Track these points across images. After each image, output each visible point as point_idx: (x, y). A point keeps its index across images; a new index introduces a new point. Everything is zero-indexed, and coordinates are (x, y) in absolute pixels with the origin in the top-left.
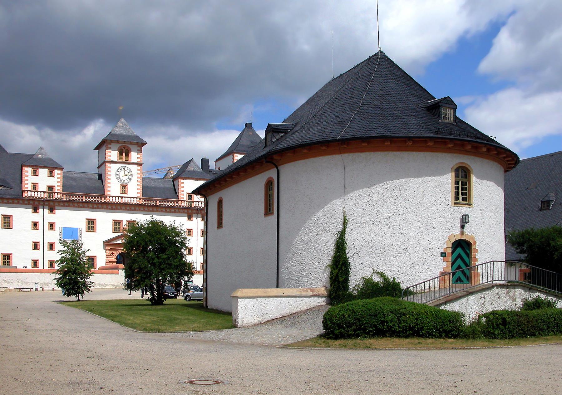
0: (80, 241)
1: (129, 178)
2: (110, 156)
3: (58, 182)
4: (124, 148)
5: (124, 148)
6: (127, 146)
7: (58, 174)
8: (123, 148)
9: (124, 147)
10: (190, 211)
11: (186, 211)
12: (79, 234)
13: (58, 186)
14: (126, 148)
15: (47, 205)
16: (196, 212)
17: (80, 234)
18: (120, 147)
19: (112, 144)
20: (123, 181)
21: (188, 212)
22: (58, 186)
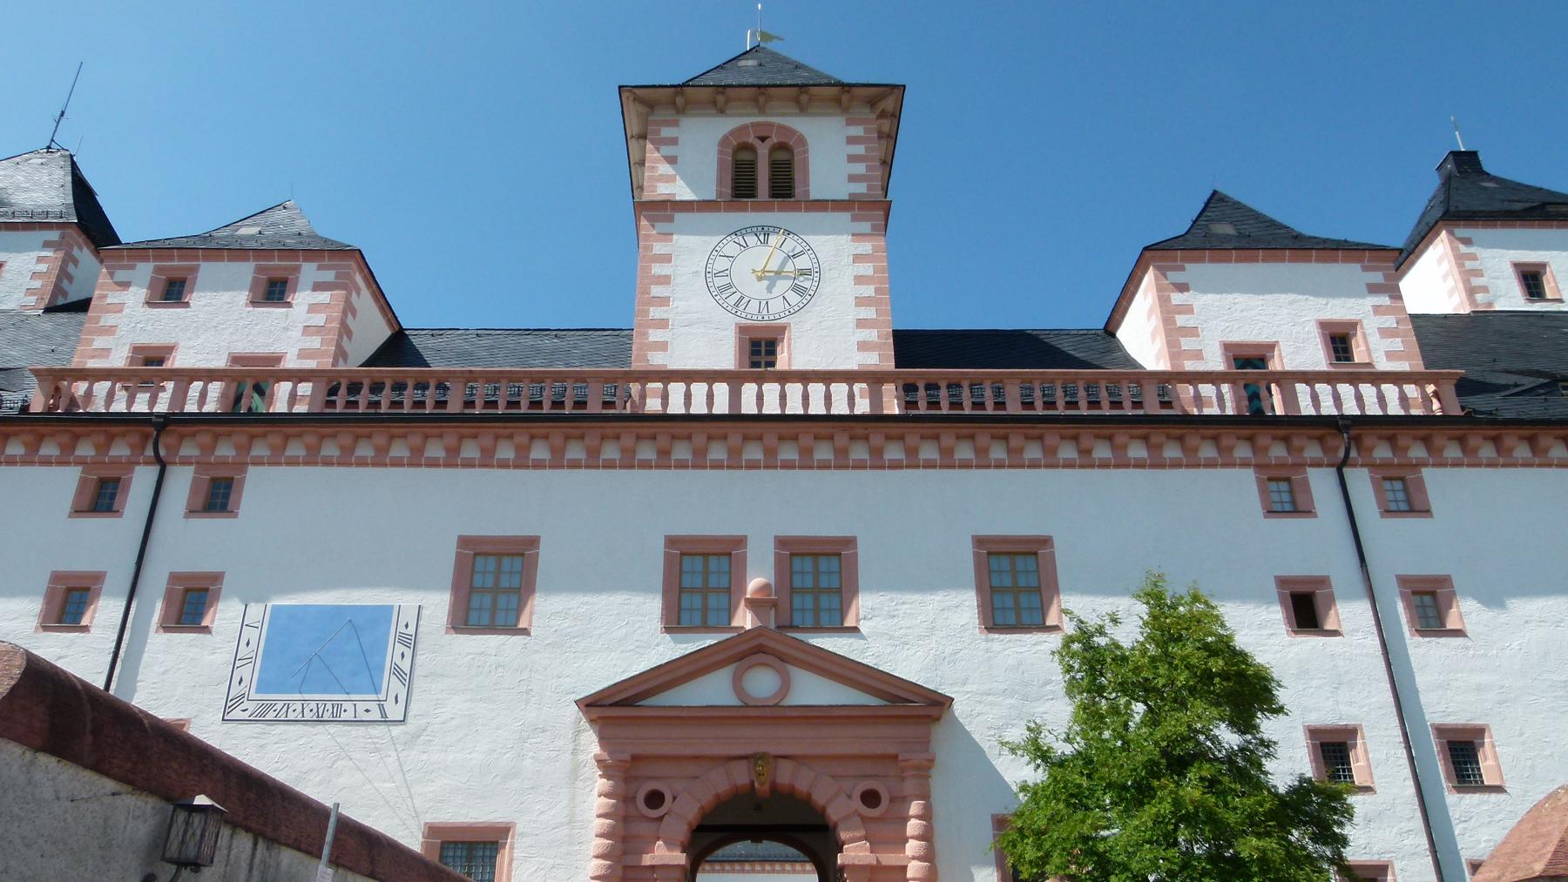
1: (798, 289)
4: (763, 139)
5: (763, 139)
6: (781, 127)
8: (751, 139)
9: (763, 134)
12: (395, 653)
14: (775, 140)
15: (186, 462)
17: (400, 648)
18: (732, 133)
20: (753, 307)
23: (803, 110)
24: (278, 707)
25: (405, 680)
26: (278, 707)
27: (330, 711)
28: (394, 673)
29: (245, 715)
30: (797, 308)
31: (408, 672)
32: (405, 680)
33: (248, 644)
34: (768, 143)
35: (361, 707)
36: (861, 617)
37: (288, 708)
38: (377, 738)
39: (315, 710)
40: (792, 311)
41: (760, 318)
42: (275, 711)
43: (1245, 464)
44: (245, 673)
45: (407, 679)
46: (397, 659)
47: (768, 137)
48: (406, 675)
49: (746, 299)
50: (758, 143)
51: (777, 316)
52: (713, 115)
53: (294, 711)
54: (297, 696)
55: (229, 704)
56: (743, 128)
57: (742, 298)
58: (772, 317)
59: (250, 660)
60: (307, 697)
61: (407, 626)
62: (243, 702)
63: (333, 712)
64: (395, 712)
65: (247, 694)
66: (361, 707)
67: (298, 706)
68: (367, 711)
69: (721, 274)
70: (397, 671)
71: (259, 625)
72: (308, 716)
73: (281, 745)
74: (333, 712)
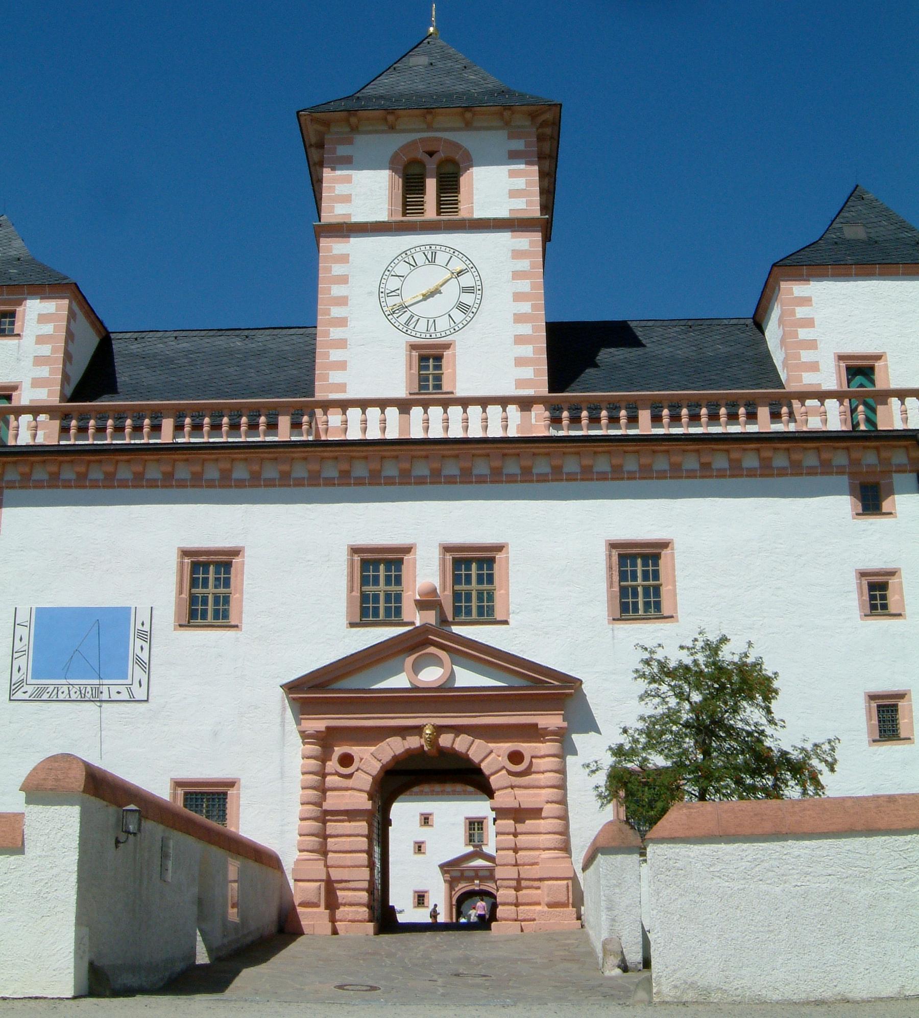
0: (135, 688)
1: (462, 307)
2: (347, 199)
3: (39, 361)
4: (431, 154)
6: (447, 142)
7: (43, 319)
8: (420, 155)
9: (431, 149)
10: (870, 458)
11: (840, 459)
12: (135, 645)
13: (37, 383)
14: (441, 155)
16: (909, 459)
17: (139, 642)
18: (405, 148)
19: (360, 139)
20: (422, 326)
21: (855, 462)
22: (37, 383)
23: (468, 126)
24: (51, 688)
25: (146, 668)
26: (51, 688)
27: (90, 692)
28: (136, 662)
29: (26, 697)
30: (461, 326)
31: (147, 661)
32: (146, 668)
33: (21, 640)
34: (436, 158)
35: (114, 689)
36: (510, 611)
37: (58, 691)
38: (128, 713)
39: (78, 692)
40: (457, 329)
41: (428, 336)
42: (48, 693)
43: (841, 472)
44: (22, 662)
45: (146, 666)
46: (138, 651)
47: (436, 152)
48: (146, 664)
49: (416, 318)
50: (426, 158)
51: (443, 334)
52: (383, 132)
53: (63, 693)
54: (64, 681)
55: (13, 688)
56: (414, 143)
57: (412, 317)
58: (438, 335)
59: (24, 653)
60: (71, 681)
61: (143, 624)
62: (23, 686)
63: (92, 694)
64: (140, 694)
65: (25, 679)
66: (114, 689)
67: (65, 688)
68: (119, 693)
69: (394, 294)
70: (139, 661)
71: (28, 624)
72: (74, 697)
73: (55, 719)
74: (92, 694)
